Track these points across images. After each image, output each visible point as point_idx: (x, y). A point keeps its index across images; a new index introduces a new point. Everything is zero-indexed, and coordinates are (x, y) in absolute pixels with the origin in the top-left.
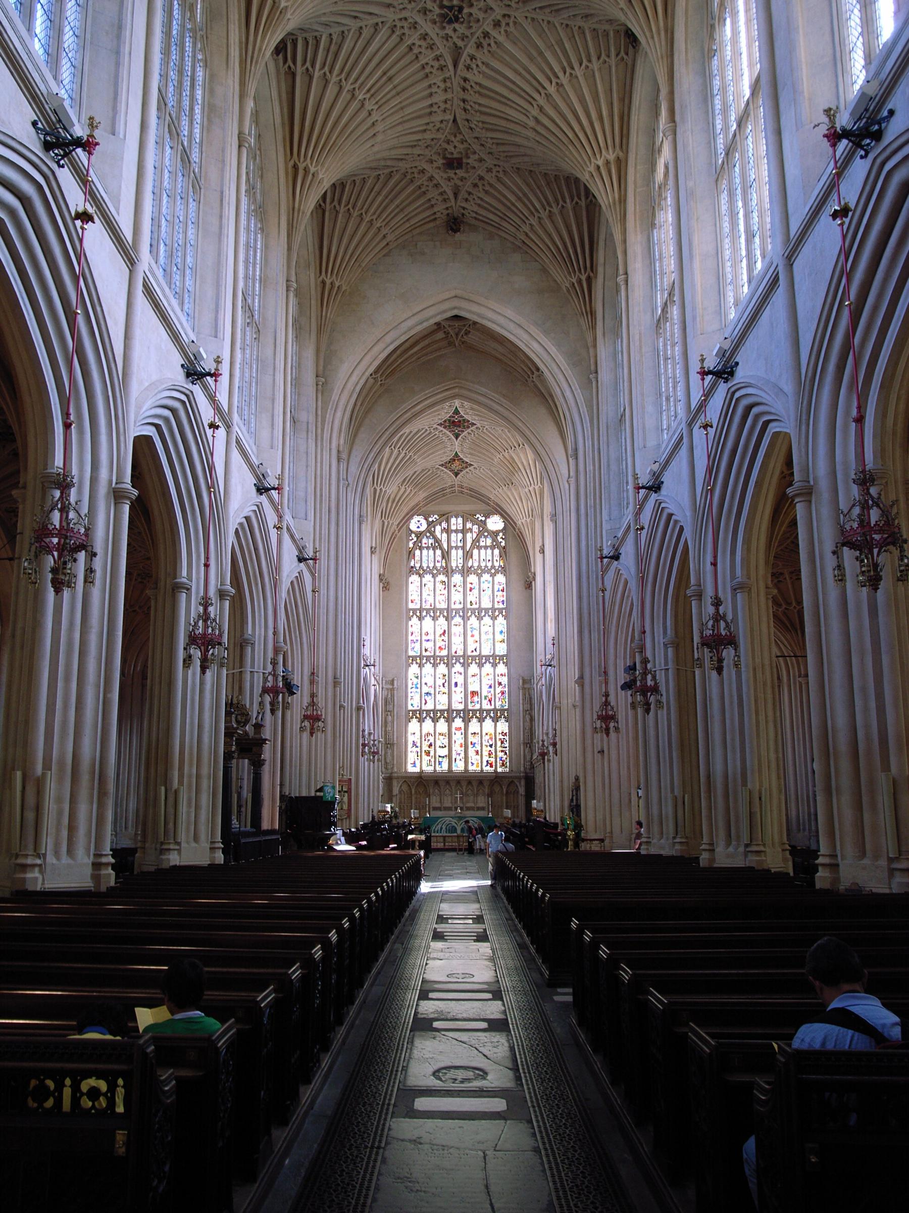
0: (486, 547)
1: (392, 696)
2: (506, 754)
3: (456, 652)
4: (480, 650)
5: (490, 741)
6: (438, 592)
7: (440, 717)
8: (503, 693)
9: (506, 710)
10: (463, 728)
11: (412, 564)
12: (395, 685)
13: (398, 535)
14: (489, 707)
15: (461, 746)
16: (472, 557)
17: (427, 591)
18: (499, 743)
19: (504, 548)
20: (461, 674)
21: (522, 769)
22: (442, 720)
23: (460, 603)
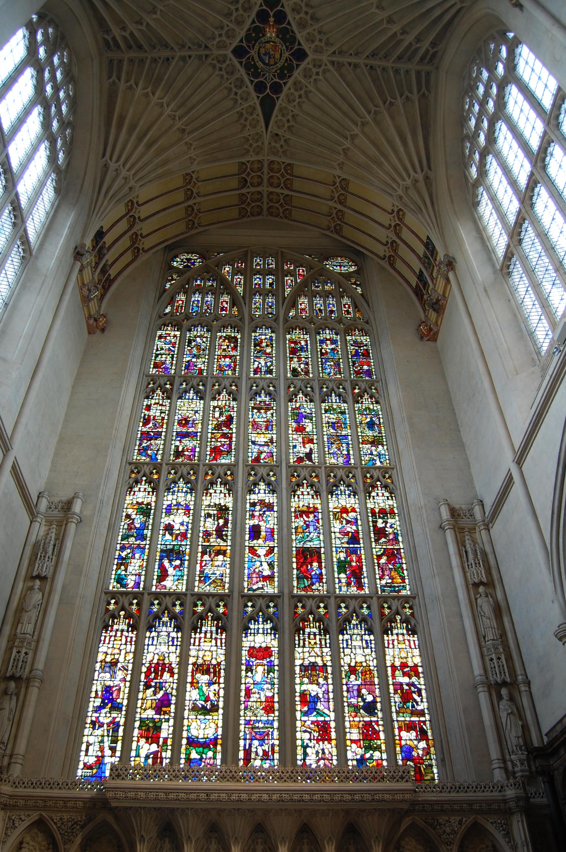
0: (326, 295)
1: (61, 540)
2: (423, 735)
3: (257, 459)
4: (322, 455)
5: (364, 691)
6: (218, 352)
7: (202, 617)
8: (392, 555)
9: (406, 599)
10: (275, 650)
11: (168, 310)
12: (77, 507)
13: (143, 257)
14: (353, 590)
15: (269, 710)
16: (294, 305)
17: (195, 351)
18: (397, 698)
19: (362, 295)
20: (270, 507)
21: (498, 775)
22: (208, 627)
23: (270, 372)
